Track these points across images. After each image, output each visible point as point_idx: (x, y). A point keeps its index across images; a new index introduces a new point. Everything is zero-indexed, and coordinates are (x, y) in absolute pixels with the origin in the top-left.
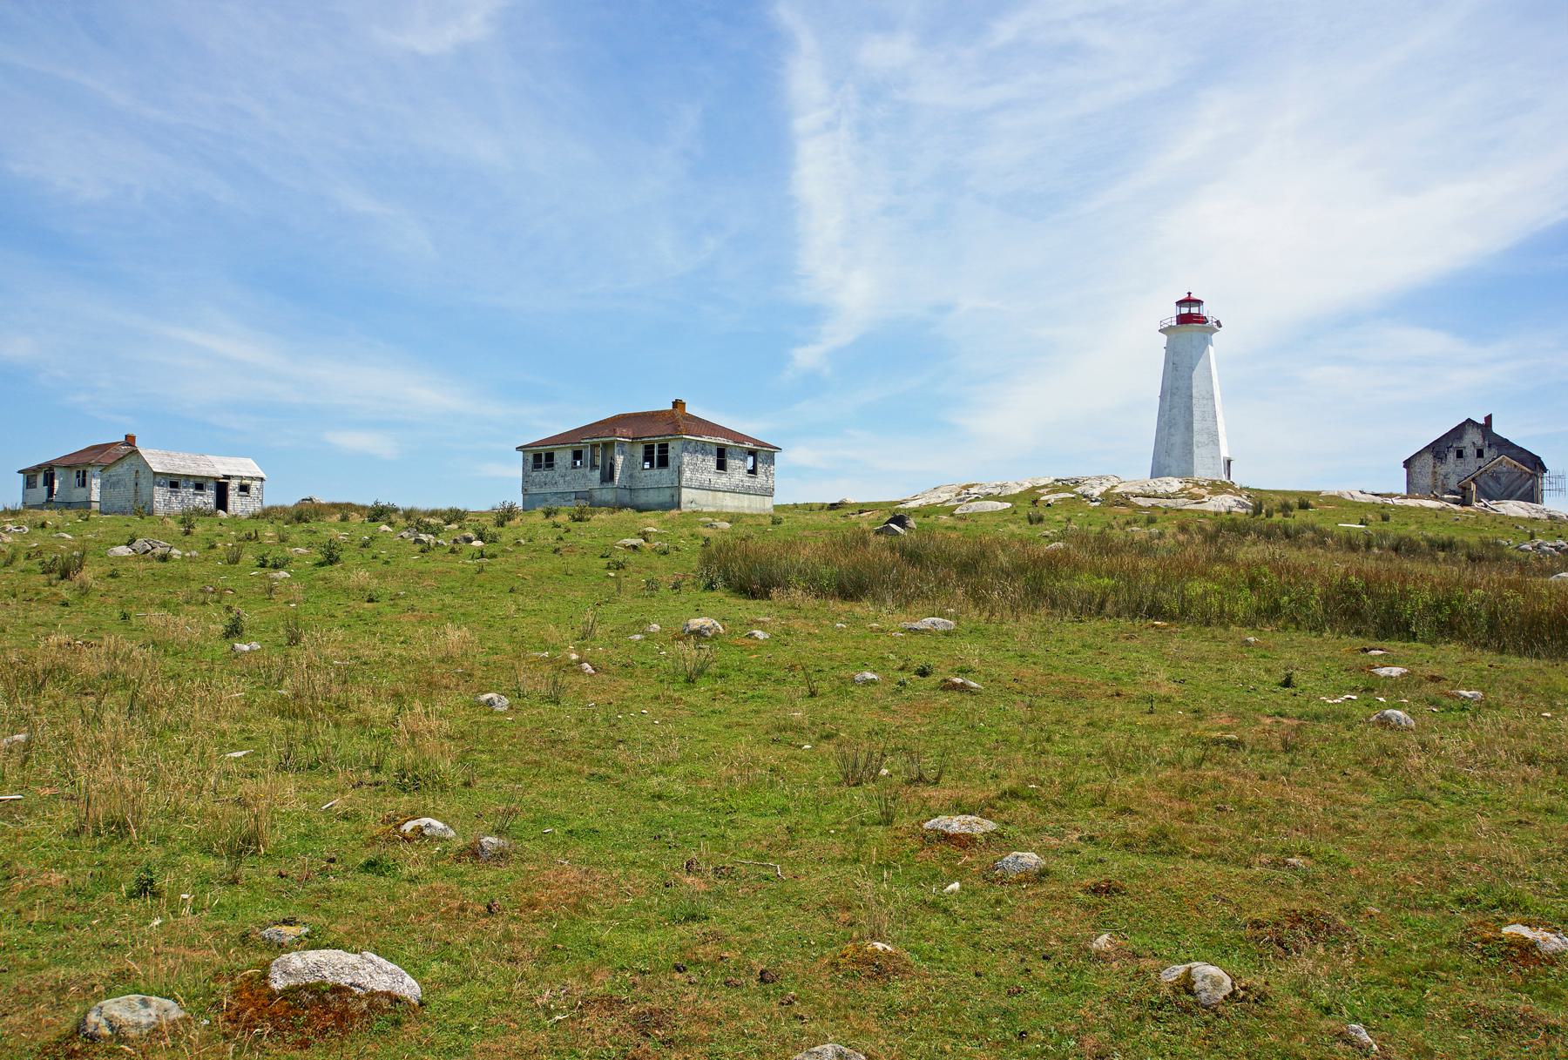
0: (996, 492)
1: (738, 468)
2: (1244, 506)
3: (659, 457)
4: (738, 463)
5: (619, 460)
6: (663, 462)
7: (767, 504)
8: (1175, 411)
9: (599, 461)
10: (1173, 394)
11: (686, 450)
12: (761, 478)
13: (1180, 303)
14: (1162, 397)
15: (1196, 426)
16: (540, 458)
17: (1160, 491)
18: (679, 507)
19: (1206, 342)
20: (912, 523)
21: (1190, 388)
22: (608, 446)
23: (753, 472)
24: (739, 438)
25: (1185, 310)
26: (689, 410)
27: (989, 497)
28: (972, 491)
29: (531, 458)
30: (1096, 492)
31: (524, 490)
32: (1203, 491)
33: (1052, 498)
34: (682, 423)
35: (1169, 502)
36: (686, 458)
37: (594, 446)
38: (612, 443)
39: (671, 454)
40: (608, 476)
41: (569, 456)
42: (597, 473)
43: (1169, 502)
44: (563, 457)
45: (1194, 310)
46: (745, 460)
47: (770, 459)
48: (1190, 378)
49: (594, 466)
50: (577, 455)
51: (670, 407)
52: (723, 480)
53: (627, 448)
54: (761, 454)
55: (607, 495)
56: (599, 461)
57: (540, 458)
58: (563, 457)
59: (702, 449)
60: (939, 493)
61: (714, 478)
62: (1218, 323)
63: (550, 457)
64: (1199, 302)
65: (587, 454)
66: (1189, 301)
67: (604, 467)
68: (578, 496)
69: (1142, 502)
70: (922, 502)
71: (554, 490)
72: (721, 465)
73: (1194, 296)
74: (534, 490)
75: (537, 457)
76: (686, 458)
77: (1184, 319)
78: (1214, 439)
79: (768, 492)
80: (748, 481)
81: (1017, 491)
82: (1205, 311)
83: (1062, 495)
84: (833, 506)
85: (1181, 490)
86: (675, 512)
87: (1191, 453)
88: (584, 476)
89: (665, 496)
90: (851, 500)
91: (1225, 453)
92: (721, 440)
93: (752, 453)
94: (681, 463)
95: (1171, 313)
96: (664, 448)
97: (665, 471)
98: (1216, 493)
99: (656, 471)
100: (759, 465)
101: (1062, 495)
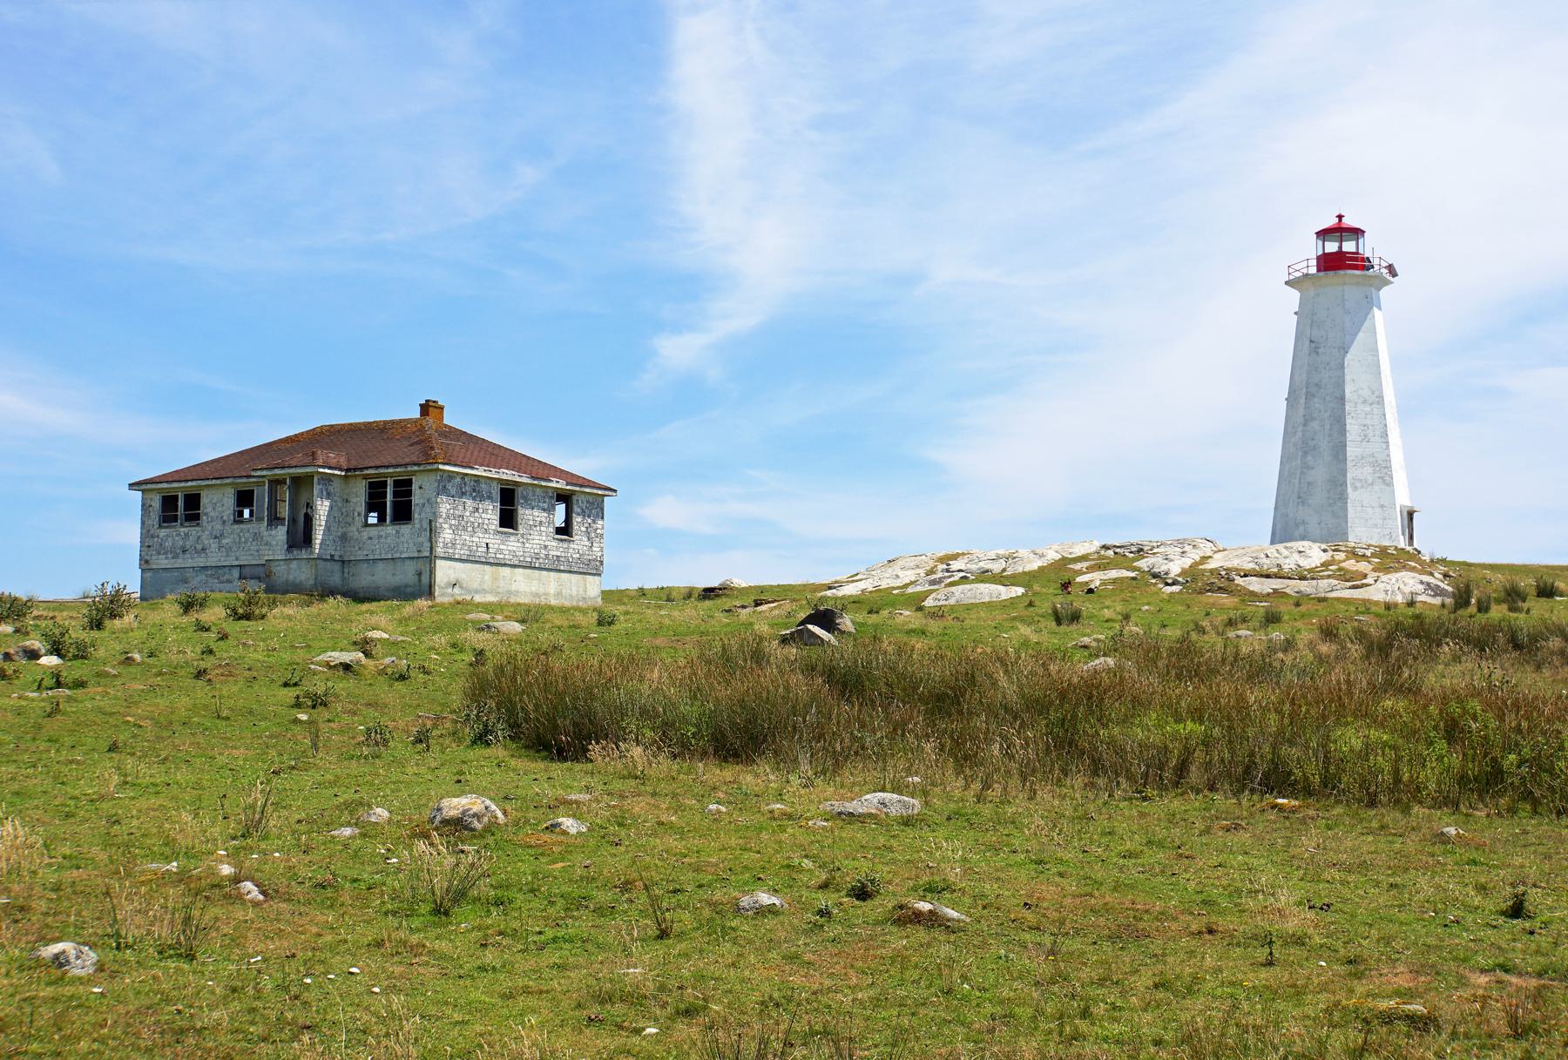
0: (996, 567)
1: (539, 522)
2: (1438, 592)
3: (394, 501)
4: (540, 515)
5: (322, 508)
6: (403, 513)
7: (590, 589)
8: (1315, 425)
9: (284, 510)
10: (1309, 396)
11: (442, 490)
12: (579, 542)
13: (1323, 234)
14: (1291, 400)
15: (1352, 451)
16: (174, 503)
17: (1289, 565)
18: (429, 592)
19: (1370, 303)
20: (846, 622)
21: (1340, 384)
22: (301, 483)
23: (565, 531)
24: (541, 470)
25: (1332, 247)
26: (449, 420)
27: (985, 576)
28: (955, 565)
29: (157, 503)
30: (1175, 568)
31: (145, 562)
32: (1363, 566)
33: (1096, 579)
34: (437, 441)
35: (1304, 586)
36: (445, 506)
37: (276, 483)
38: (310, 477)
39: (417, 499)
40: (301, 537)
41: (228, 500)
42: (281, 533)
43: (1304, 586)
44: (219, 503)
45: (1349, 246)
46: (550, 510)
47: (596, 508)
48: (1343, 367)
49: (274, 520)
50: (244, 498)
51: (416, 414)
52: (509, 546)
53: (336, 486)
54: (577, 500)
55: (300, 572)
56: (284, 510)
57: (174, 503)
58: (219, 503)
59: (474, 489)
60: (896, 569)
61: (495, 542)
62: (1391, 269)
63: (193, 501)
64: (1357, 233)
65: (262, 496)
66: (1339, 231)
67: (293, 521)
68: (245, 572)
69: (1255, 585)
70: (867, 585)
71: (200, 561)
72: (508, 520)
73: (1347, 222)
74: (162, 562)
75: (169, 502)
76: (445, 506)
77: (1330, 263)
78: (1385, 478)
79: (593, 568)
80: (556, 548)
81: (1035, 565)
82: (1367, 247)
83: (1113, 574)
84: (709, 593)
85: (1325, 565)
86: (422, 603)
87: (1342, 498)
88: (257, 537)
89: (406, 575)
90: (740, 582)
91: (1403, 498)
92: (507, 475)
93: (564, 497)
94: (435, 515)
95: (1307, 252)
96: (404, 488)
97: (405, 529)
98: (1387, 570)
99: (390, 529)
100: (577, 519)
101: (1113, 574)
